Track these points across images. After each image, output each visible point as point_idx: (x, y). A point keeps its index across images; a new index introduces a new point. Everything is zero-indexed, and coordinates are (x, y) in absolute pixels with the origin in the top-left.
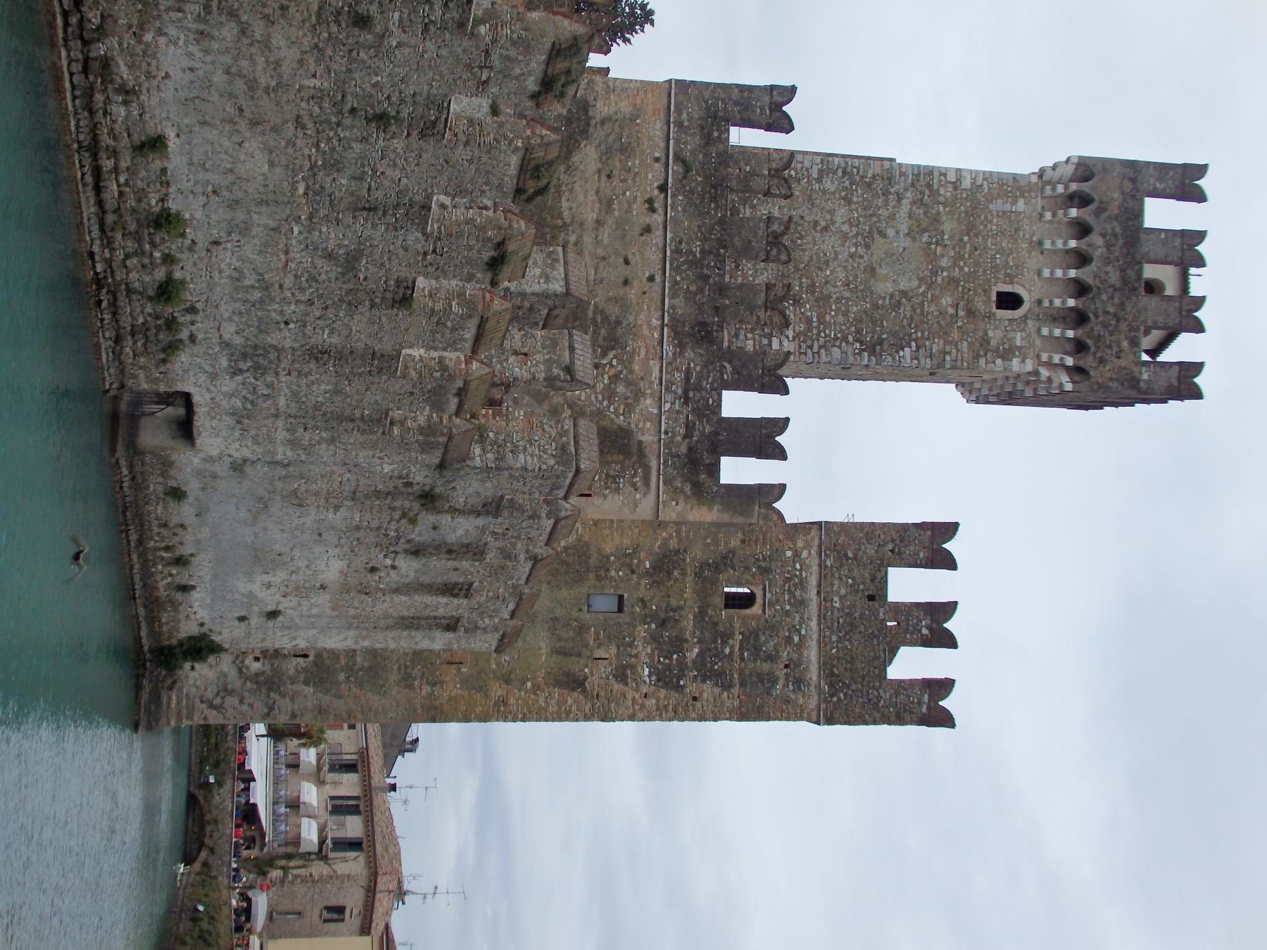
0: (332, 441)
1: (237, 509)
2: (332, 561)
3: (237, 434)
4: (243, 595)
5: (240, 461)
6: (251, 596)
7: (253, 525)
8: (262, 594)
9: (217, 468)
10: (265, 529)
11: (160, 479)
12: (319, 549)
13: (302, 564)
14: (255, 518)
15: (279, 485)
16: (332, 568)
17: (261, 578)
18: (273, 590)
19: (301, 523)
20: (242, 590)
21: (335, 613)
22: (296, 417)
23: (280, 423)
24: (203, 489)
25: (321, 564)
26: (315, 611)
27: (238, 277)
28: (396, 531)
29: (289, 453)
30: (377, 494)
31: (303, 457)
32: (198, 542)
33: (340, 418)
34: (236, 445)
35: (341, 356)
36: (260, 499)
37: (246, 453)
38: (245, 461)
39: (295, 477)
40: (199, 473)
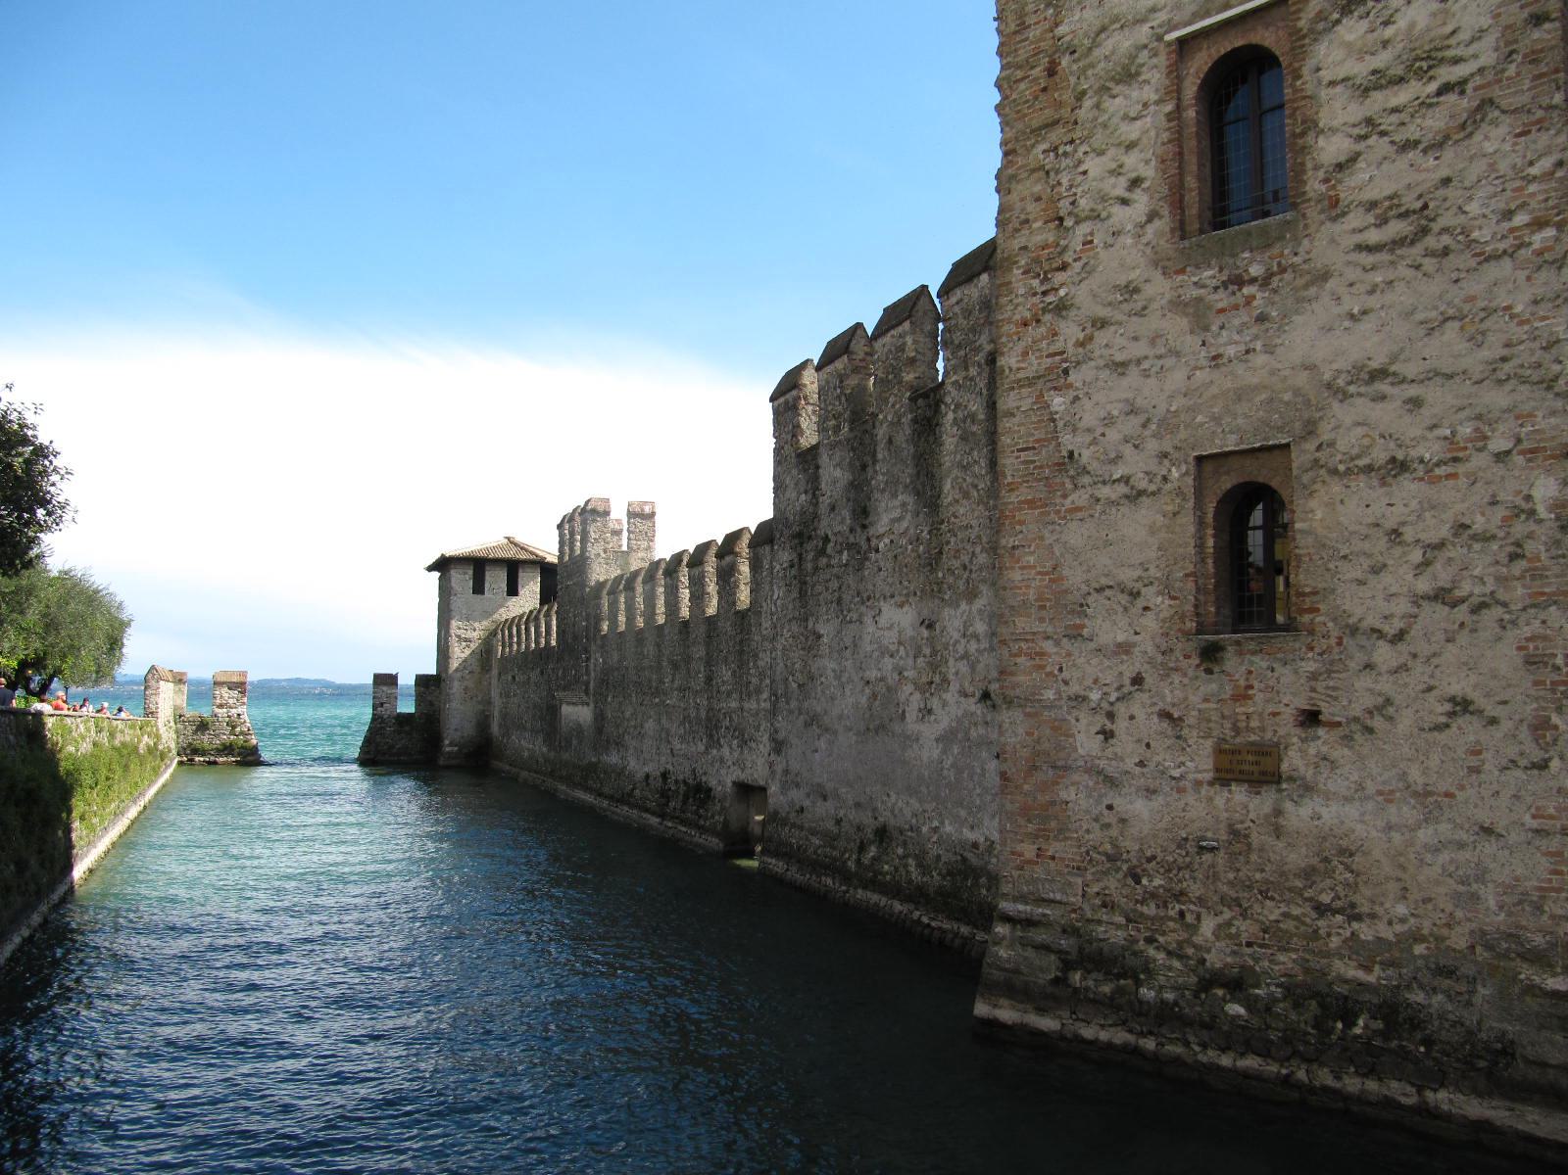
0: (756, 656)
1: (816, 751)
2: (883, 621)
3: (753, 745)
4: (944, 752)
5: (773, 745)
6: (946, 739)
7: (835, 733)
8: (943, 720)
9: (779, 768)
10: (840, 717)
11: (787, 829)
12: (867, 647)
13: (888, 663)
14: (827, 730)
15: (794, 704)
16: (897, 619)
17: (912, 724)
18: (935, 703)
19: (832, 674)
20: (936, 753)
21: (984, 588)
22: (741, 693)
23: (746, 705)
24: (798, 786)
25: (890, 638)
26: (980, 627)
27: (682, 738)
28: (840, 552)
29: (765, 695)
30: (802, 594)
31: (768, 681)
32: (858, 805)
33: (741, 652)
34: (761, 746)
35: (709, 663)
36: (807, 725)
37: (765, 739)
38: (773, 740)
39: (787, 687)
40: (785, 788)
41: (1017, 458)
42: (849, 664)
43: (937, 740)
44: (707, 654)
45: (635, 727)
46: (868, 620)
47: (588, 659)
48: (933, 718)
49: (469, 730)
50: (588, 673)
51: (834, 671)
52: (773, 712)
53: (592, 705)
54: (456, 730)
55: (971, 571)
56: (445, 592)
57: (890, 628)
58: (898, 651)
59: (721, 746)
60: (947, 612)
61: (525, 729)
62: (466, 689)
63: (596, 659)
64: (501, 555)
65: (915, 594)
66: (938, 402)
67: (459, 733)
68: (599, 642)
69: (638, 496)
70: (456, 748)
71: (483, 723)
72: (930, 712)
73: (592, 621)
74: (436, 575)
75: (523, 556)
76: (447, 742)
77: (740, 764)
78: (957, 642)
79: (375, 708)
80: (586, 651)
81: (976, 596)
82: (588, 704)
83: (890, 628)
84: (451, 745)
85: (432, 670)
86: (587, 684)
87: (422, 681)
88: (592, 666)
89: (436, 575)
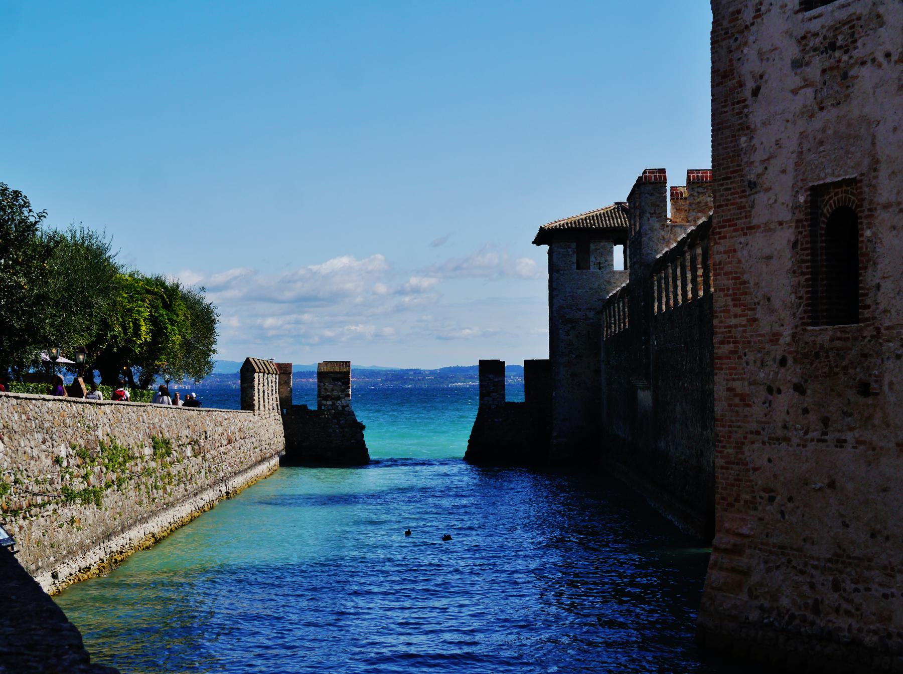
41: (722, 185)
74: (545, 248)
76: (555, 434)
79: (481, 399)
85: (544, 354)
89: (545, 248)
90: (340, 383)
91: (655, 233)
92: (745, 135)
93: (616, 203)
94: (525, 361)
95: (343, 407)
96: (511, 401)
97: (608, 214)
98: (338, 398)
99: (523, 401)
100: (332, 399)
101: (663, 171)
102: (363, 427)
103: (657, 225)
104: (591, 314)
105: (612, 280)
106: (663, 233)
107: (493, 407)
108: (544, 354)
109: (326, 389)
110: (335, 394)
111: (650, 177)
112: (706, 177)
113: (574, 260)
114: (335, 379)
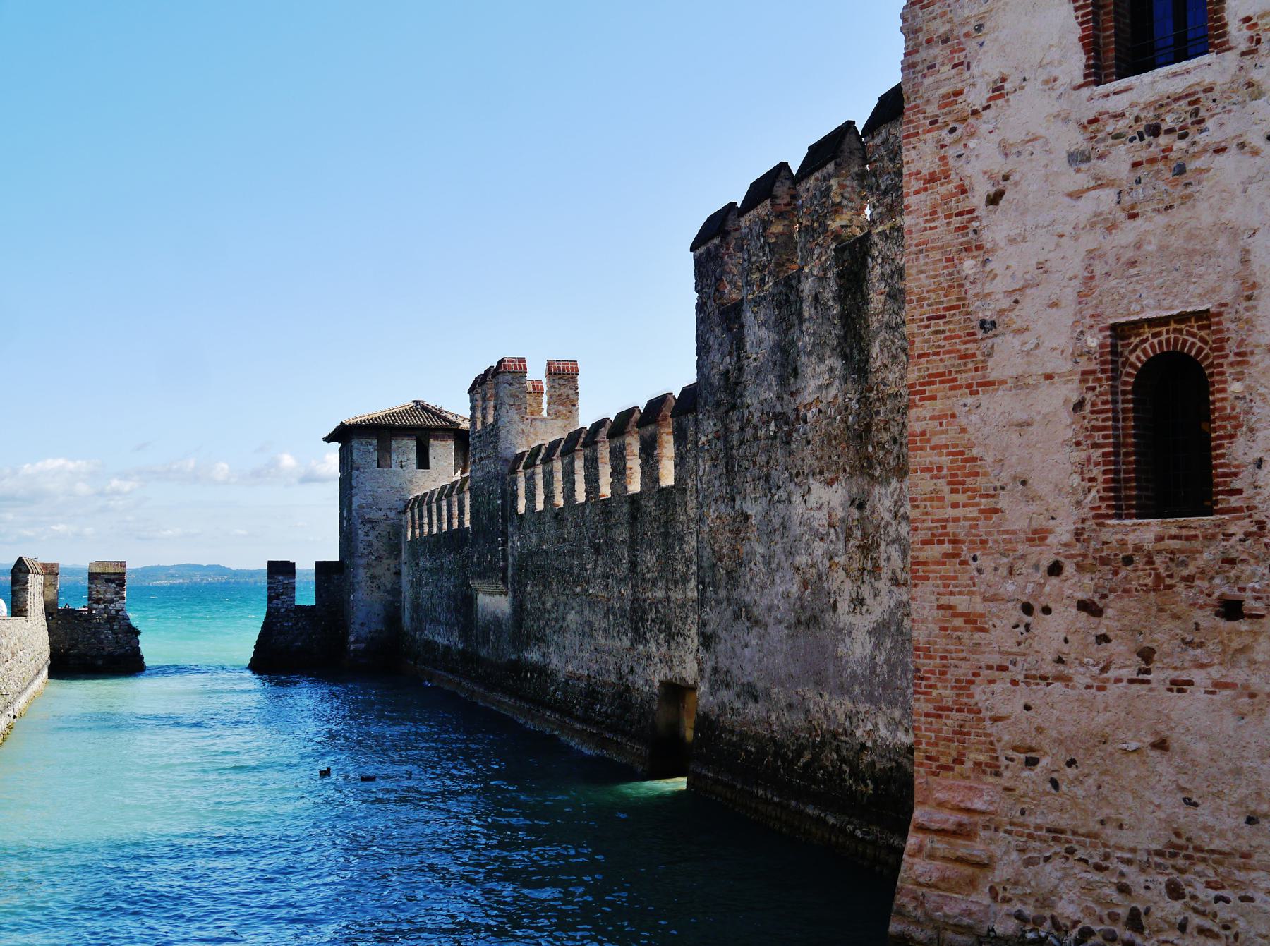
0: (681, 539)
1: (746, 646)
2: (812, 500)
3: (681, 640)
4: (877, 646)
6: (878, 631)
7: (766, 626)
9: (708, 668)
10: (770, 609)
13: (819, 548)
15: (722, 593)
17: (844, 616)
18: (866, 592)
24: (727, 686)
28: (767, 423)
29: (692, 584)
31: (694, 568)
32: (790, 706)
33: (666, 535)
34: (689, 641)
35: (633, 544)
36: (736, 617)
40: (713, 690)
41: (927, 327)
42: (778, 548)
43: (870, 633)
44: (631, 537)
45: (557, 620)
46: (797, 499)
47: (505, 543)
48: (865, 608)
49: (376, 625)
50: (505, 559)
51: (763, 556)
52: (701, 602)
53: (510, 594)
54: (362, 624)
55: (901, 444)
56: (347, 464)
57: (819, 508)
58: (828, 534)
59: (648, 642)
60: (878, 490)
61: (439, 623)
62: (373, 577)
63: (513, 542)
64: (408, 421)
65: (845, 470)
66: (866, 253)
67: (366, 629)
68: (516, 522)
69: (562, 354)
70: (363, 645)
71: (392, 615)
72: (862, 602)
73: (509, 498)
74: (337, 445)
75: (434, 423)
76: (352, 639)
77: (668, 661)
78: (888, 524)
79: (270, 599)
80: (504, 533)
81: (906, 473)
82: (506, 595)
83: (819, 508)
84: (356, 641)
85: (334, 556)
86: (505, 570)
87: (323, 568)
88: (509, 551)
90: (114, 585)
91: (515, 426)
92: (974, 257)
93: (416, 402)
94: (317, 563)
95: (117, 611)
96: (302, 604)
97: (406, 412)
98: (112, 601)
99: (314, 603)
100: (105, 602)
101: (522, 360)
102: (138, 633)
103: (516, 418)
104: (392, 514)
105: (414, 480)
106: (523, 426)
107: (283, 610)
108: (334, 556)
109: (98, 591)
110: (108, 596)
111: (509, 366)
112: (568, 368)
113: (376, 458)
114: (108, 581)
